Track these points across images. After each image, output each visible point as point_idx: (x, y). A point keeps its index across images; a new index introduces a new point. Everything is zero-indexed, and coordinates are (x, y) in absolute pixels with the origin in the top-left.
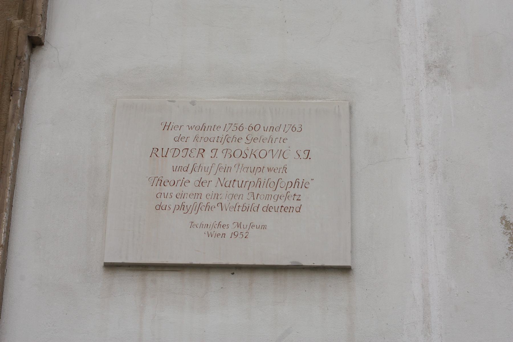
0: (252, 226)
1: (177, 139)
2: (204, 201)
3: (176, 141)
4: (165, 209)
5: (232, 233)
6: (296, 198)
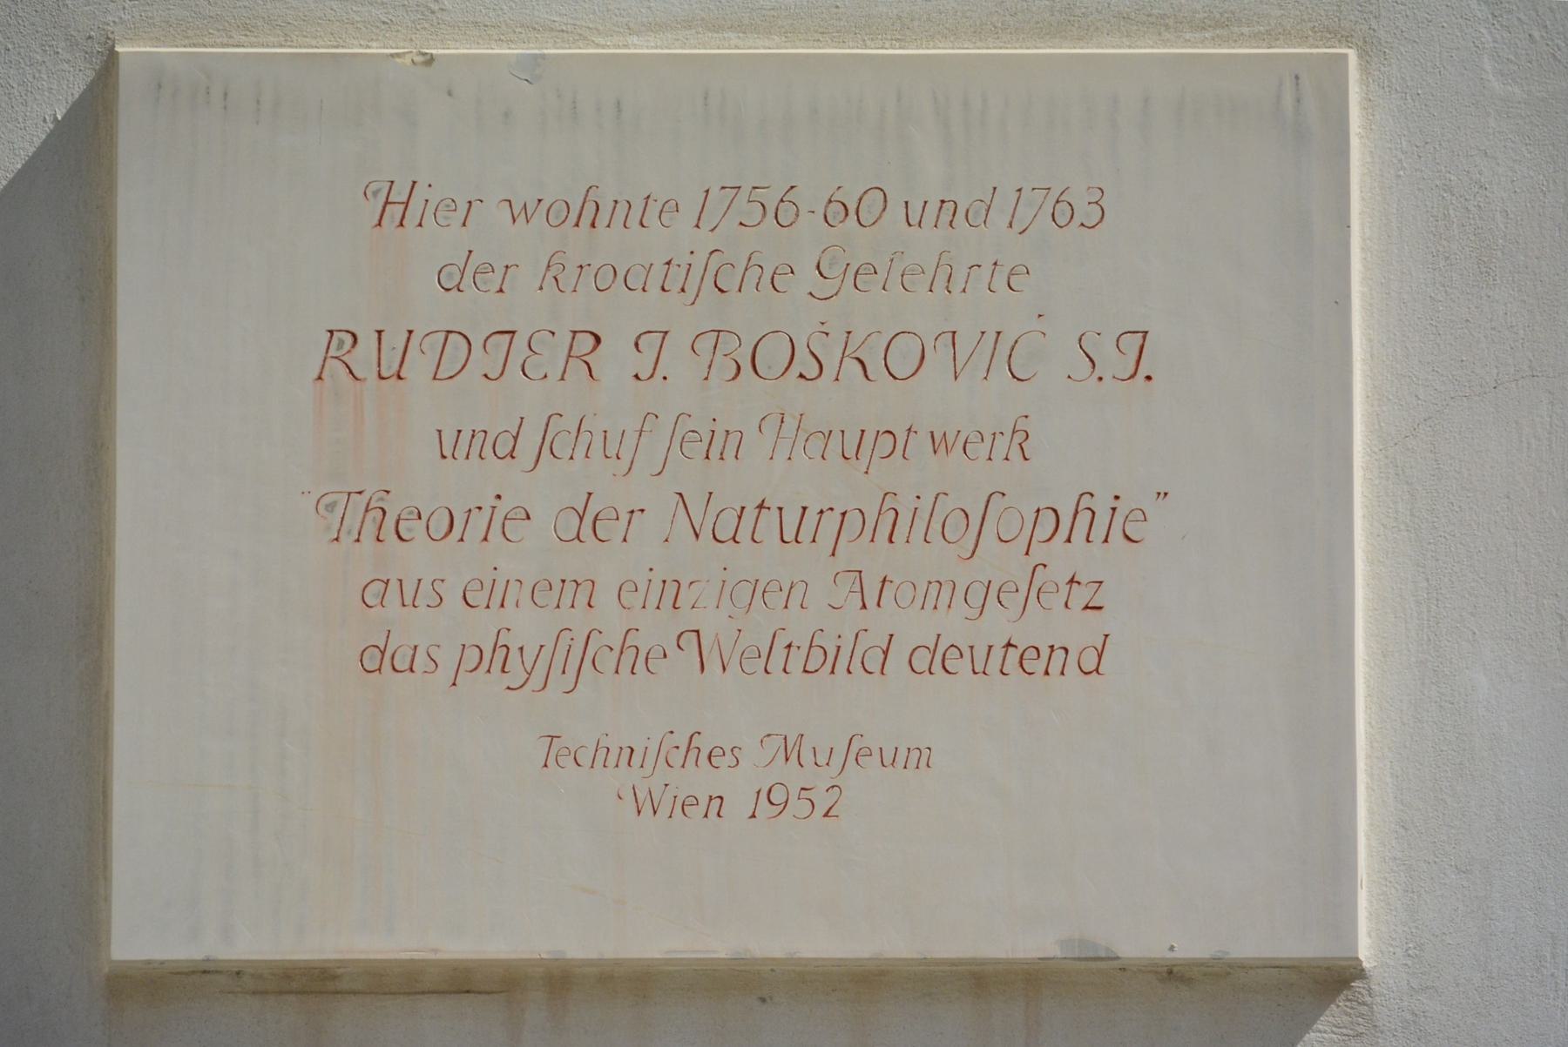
0: (855, 750)
4: (411, 670)
6: (1080, 596)
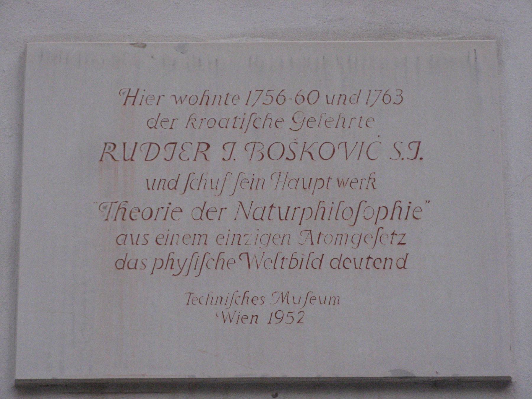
0: (310, 298)
1: (152, 122)
2: (214, 250)
3: (151, 128)
4: (135, 268)
5: (272, 314)
6: (396, 239)
